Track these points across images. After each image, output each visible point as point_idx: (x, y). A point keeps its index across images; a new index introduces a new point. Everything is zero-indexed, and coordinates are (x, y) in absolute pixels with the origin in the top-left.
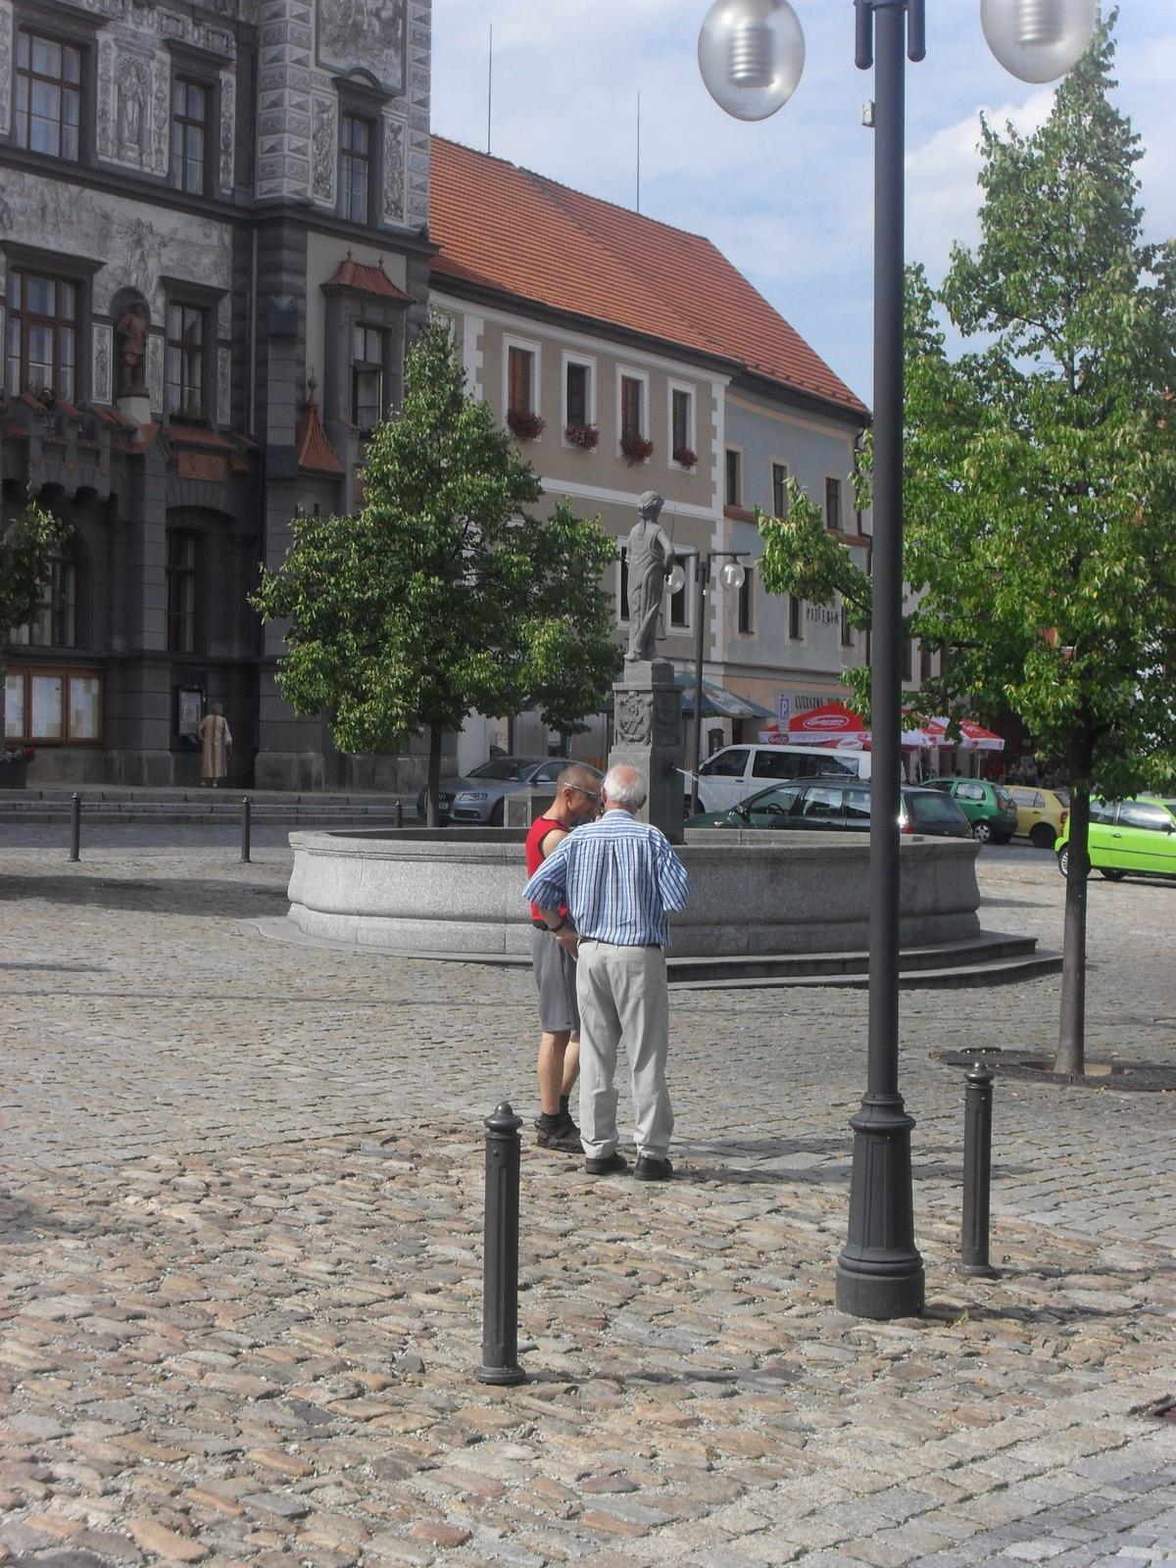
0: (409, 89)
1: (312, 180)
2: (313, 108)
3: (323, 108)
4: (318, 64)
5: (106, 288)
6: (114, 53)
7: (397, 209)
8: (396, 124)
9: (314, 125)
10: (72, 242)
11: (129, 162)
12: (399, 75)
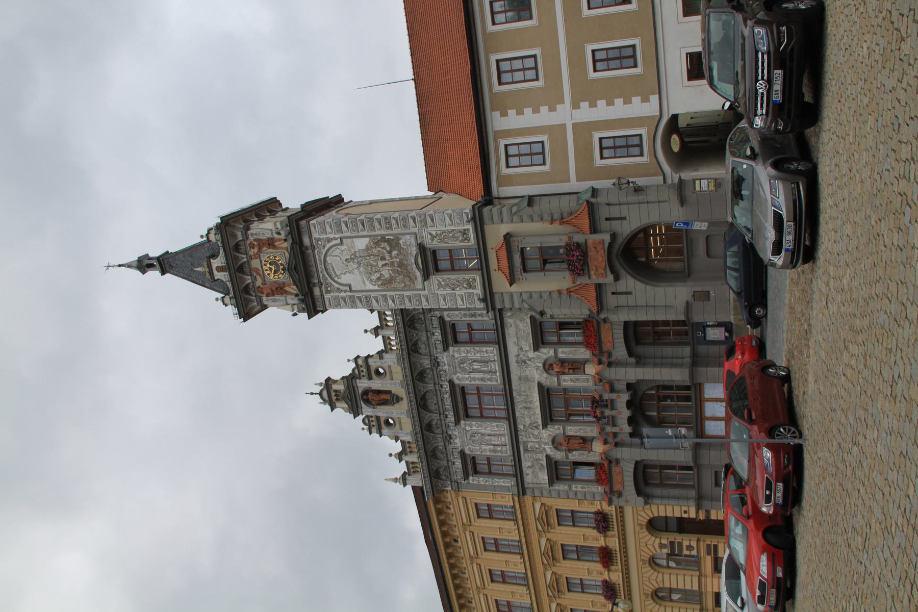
1: (471, 291)
2: (441, 292)
3: (440, 286)
5: (546, 378)
6: (458, 375)
7: (465, 233)
8: (429, 237)
10: (534, 395)
11: (496, 366)
12: (408, 237)
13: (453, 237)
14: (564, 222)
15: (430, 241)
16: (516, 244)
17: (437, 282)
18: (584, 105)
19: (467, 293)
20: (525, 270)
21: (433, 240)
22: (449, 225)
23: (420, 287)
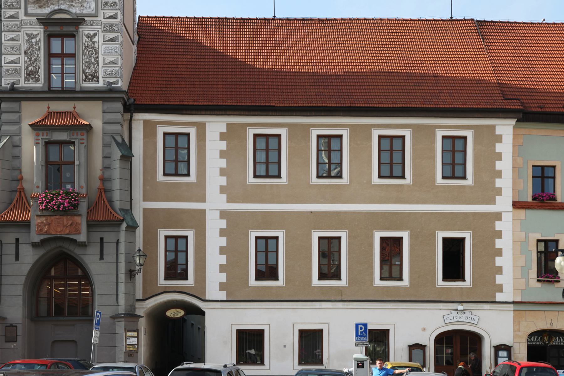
0: (101, 12)
1: (23, 74)
2: (22, 37)
4: (26, 14)
7: (94, 77)
8: (92, 33)
9: (24, 47)
13: (90, 62)
14: (101, 192)
15: (86, 33)
16: (80, 137)
17: (35, 33)
18: (223, 224)
19: (21, 69)
20: (48, 144)
21: (88, 36)
22: (104, 60)
23: (30, 10)
